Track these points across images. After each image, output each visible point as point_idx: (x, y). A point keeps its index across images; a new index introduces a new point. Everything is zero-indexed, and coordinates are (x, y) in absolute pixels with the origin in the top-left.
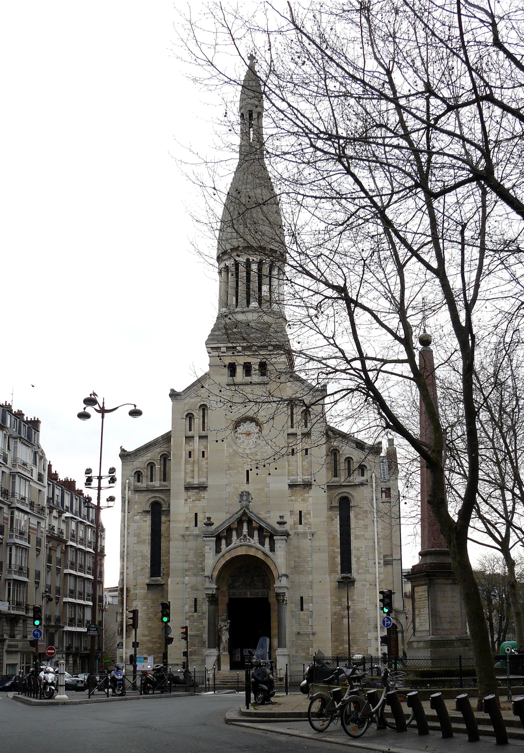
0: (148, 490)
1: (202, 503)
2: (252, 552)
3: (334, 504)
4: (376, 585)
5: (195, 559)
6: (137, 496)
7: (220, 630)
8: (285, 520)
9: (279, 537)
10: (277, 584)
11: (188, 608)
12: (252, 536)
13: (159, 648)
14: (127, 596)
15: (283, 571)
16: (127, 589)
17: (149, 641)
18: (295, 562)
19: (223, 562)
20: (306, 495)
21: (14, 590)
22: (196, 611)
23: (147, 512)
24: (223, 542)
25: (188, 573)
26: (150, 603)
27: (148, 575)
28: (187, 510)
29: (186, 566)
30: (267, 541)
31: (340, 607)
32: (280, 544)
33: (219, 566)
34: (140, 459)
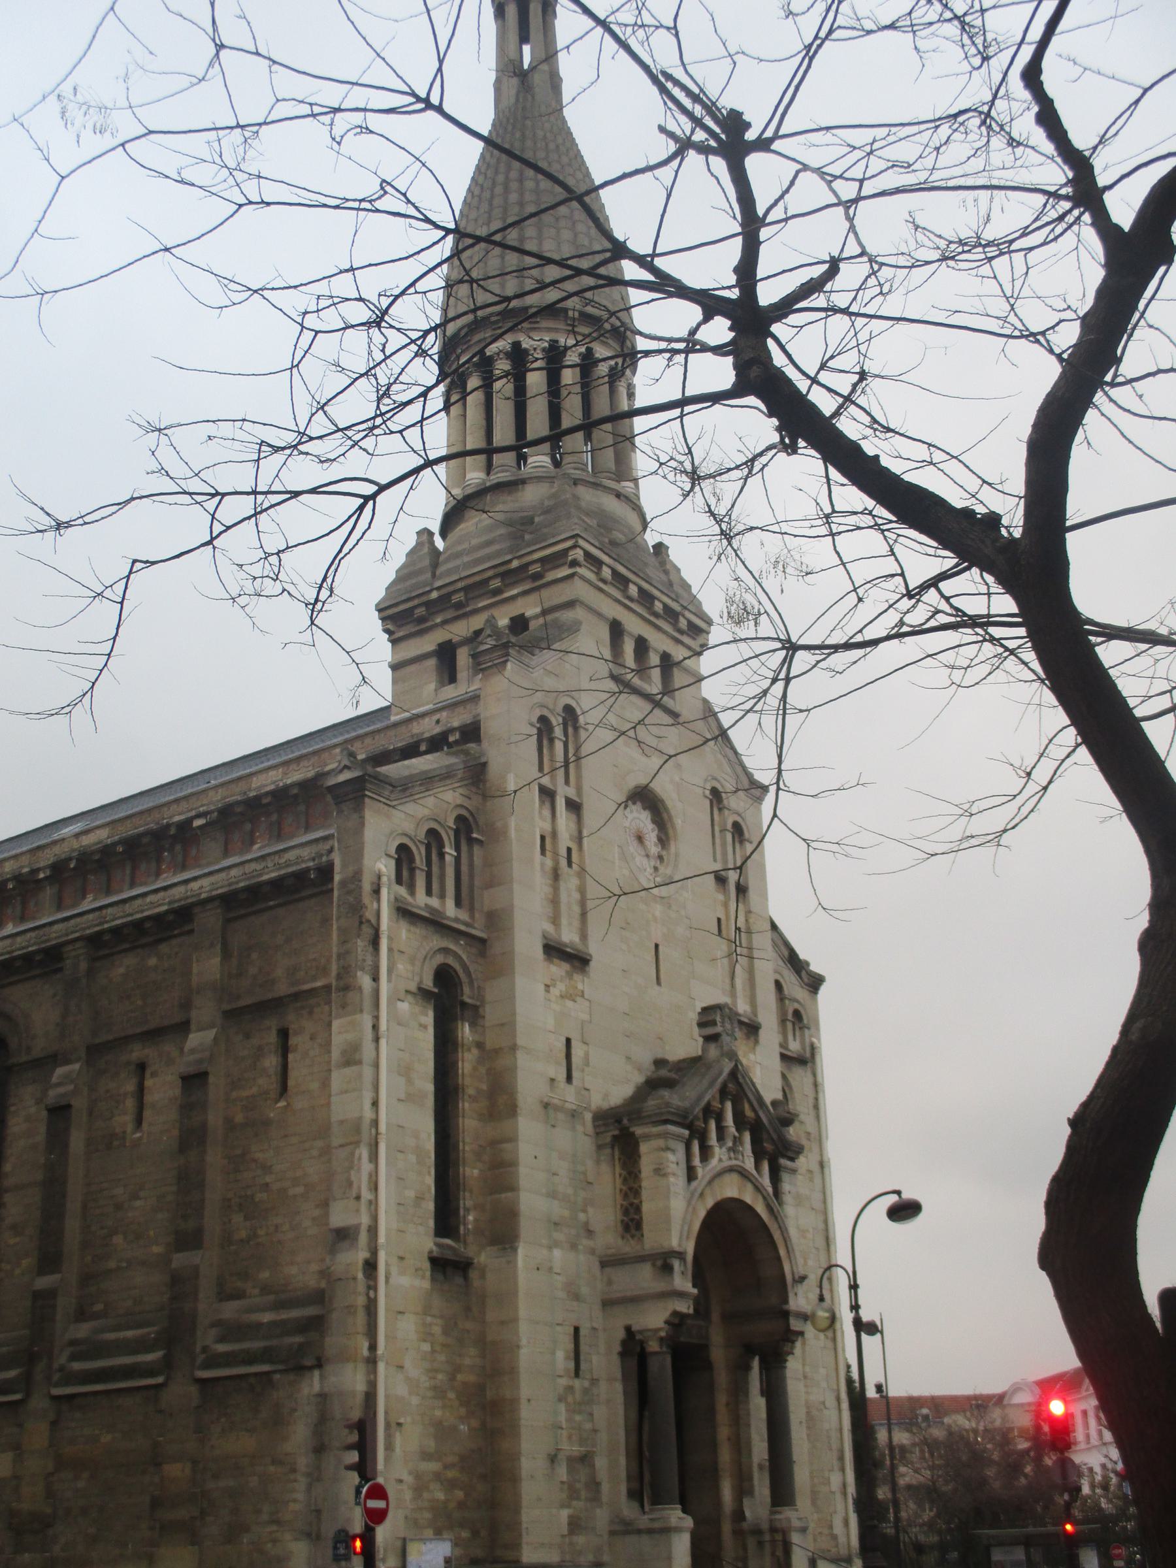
1: (578, 1010)
2: (749, 1197)
5: (570, 1191)
11: (561, 1359)
13: (461, 1505)
17: (437, 1476)
22: (577, 1373)
25: (559, 1236)
28: (550, 1023)
34: (410, 808)
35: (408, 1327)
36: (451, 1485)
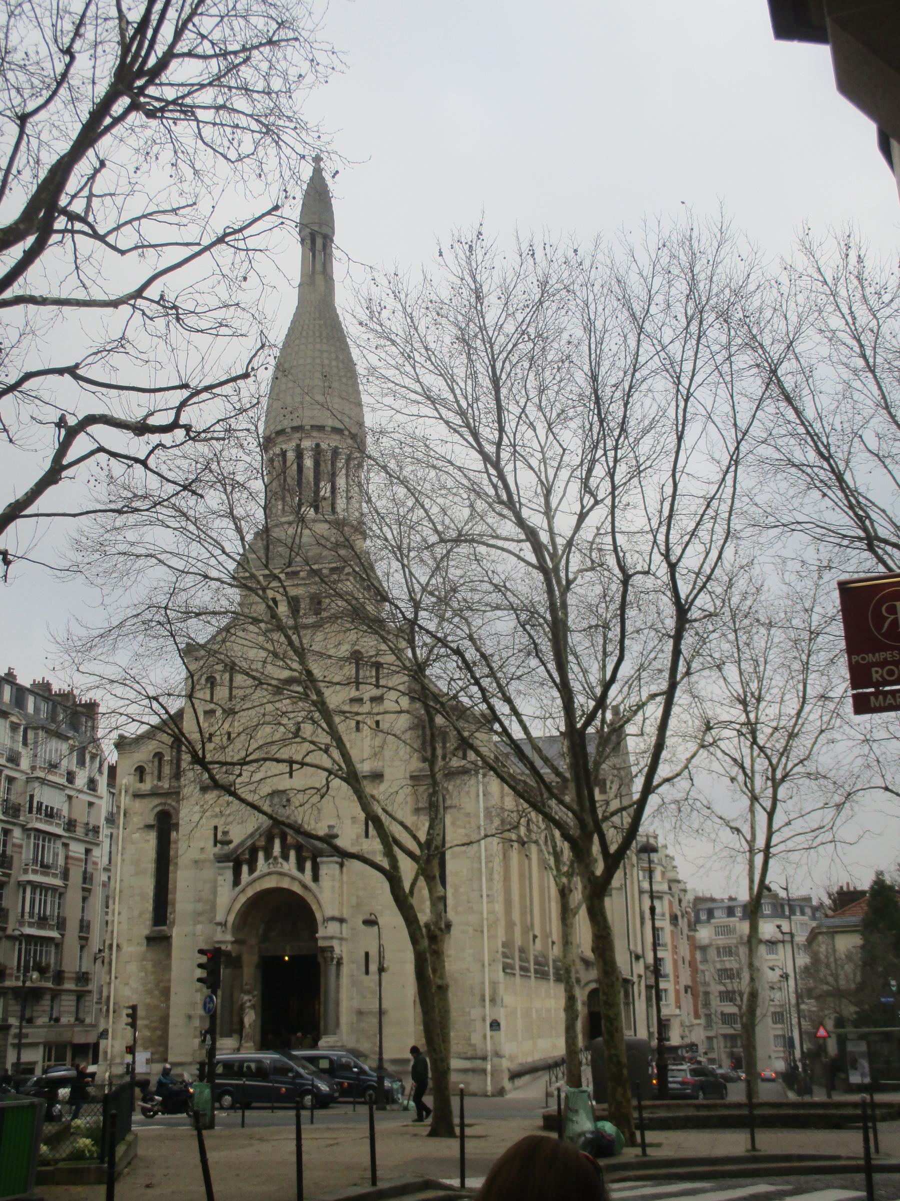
0: (153, 794)
2: (285, 884)
3: (421, 805)
4: (482, 932)
6: (138, 804)
7: (242, 1008)
8: (335, 831)
9: (325, 859)
10: (321, 933)
12: (286, 857)
14: (117, 957)
15: (331, 910)
16: (118, 946)
18: (358, 897)
19: (242, 899)
21: (41, 951)
23: (149, 827)
24: (245, 868)
25: (201, 919)
26: (149, 965)
27: (149, 923)
29: (200, 907)
30: (308, 865)
32: (329, 869)
33: (237, 906)
35: (133, 968)
36: (155, 1029)
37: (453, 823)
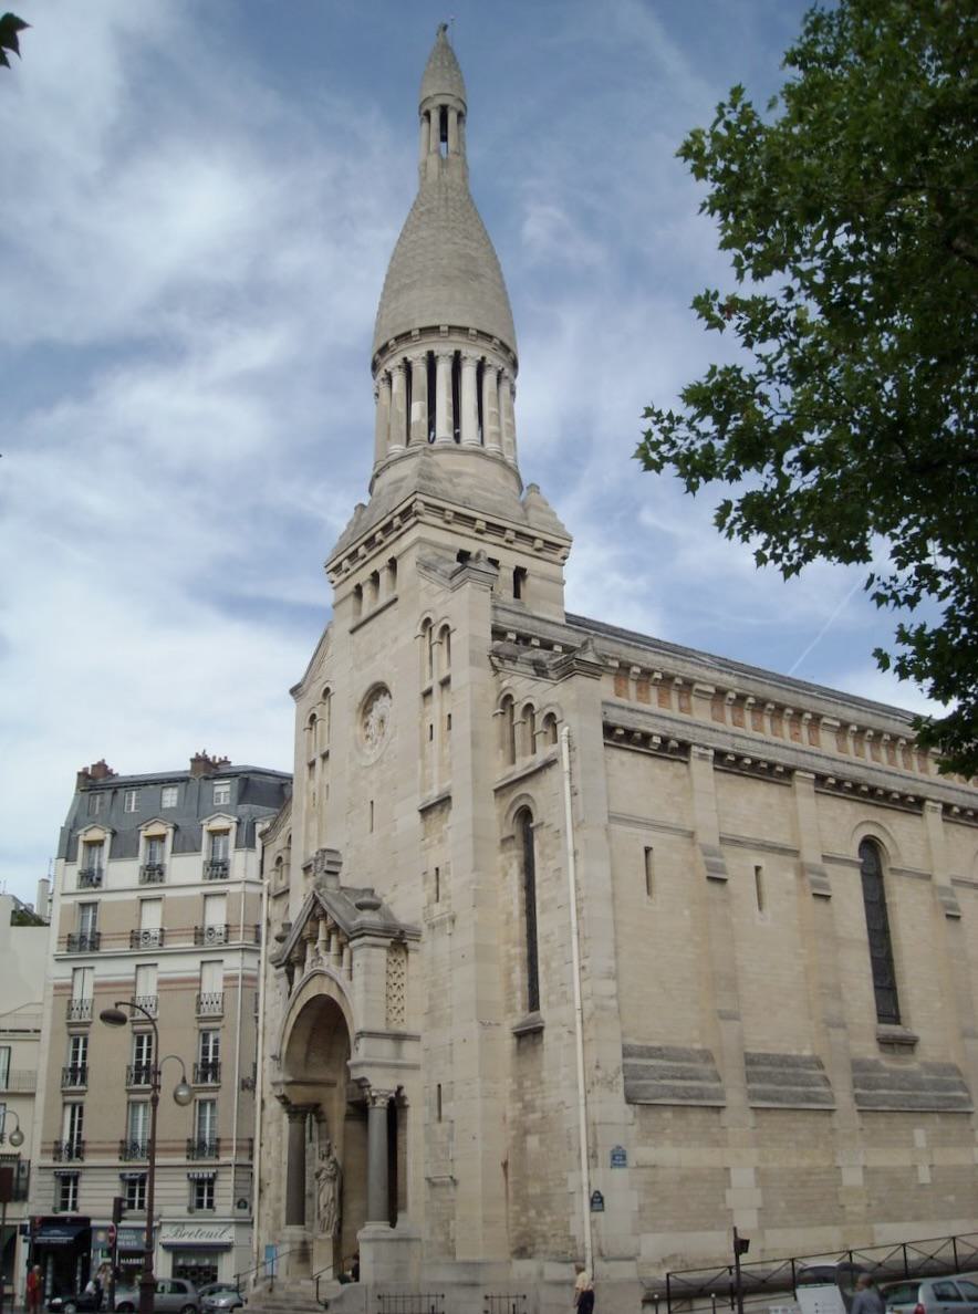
12: (328, 949)
20: (444, 827)
24: (297, 972)
31: (520, 1105)
37: (541, 853)
